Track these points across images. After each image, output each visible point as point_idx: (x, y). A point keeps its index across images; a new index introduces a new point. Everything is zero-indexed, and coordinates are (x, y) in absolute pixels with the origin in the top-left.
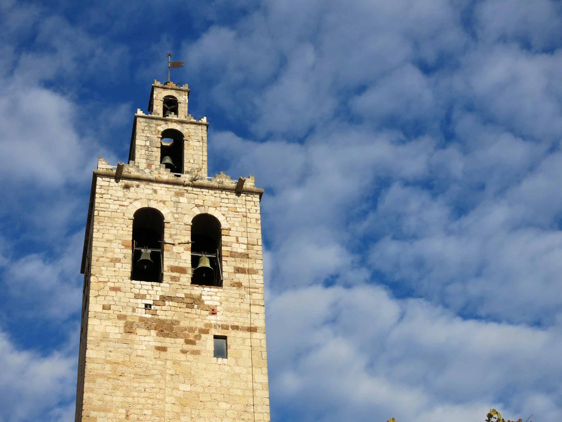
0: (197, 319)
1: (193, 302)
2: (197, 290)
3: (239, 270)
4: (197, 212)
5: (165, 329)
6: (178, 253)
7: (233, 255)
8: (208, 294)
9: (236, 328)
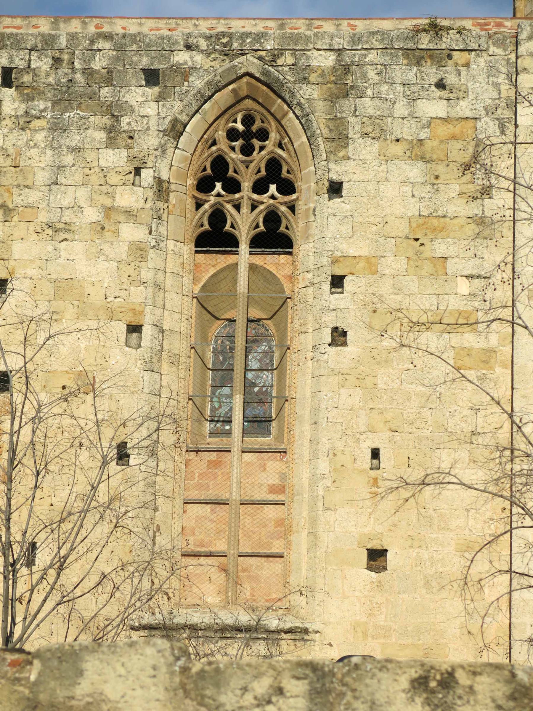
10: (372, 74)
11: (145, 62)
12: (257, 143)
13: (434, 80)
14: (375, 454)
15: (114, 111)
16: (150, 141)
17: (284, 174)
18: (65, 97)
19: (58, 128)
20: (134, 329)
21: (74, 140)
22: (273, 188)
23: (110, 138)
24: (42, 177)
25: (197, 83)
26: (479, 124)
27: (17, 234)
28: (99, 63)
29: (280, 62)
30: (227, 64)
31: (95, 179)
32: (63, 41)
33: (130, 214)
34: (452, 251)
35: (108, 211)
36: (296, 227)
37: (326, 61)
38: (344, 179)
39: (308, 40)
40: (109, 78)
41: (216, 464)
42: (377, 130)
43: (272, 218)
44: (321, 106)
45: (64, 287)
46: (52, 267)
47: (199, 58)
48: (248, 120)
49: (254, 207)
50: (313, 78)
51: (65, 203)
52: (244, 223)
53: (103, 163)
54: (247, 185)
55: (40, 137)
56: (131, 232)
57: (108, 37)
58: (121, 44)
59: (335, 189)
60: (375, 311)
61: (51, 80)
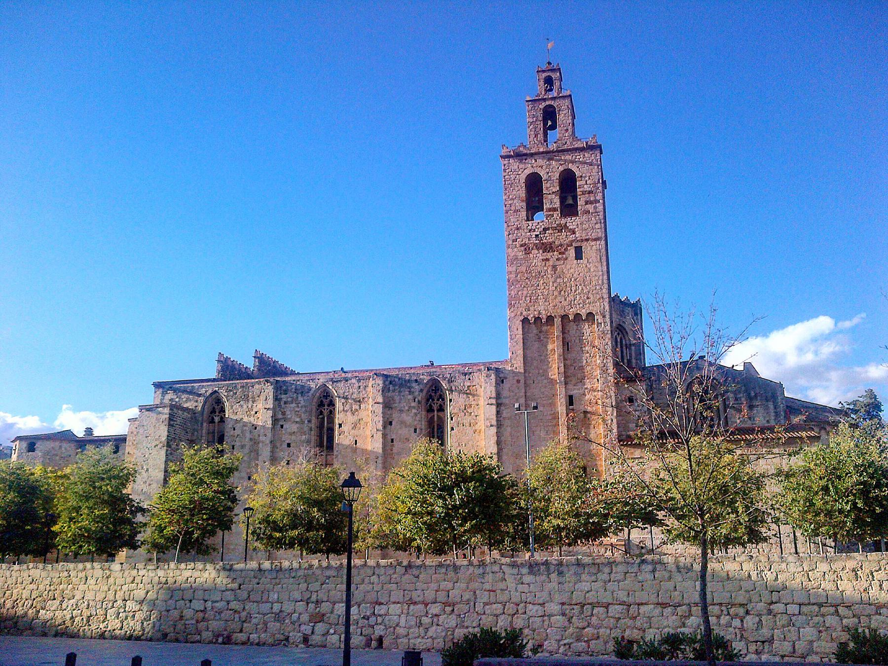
0: (564, 238)
1: (561, 228)
2: (563, 221)
3: (587, 203)
4: (561, 168)
5: (547, 248)
6: (552, 199)
7: (584, 193)
8: (572, 222)
9: (587, 240)
18: (401, 386)
20: (415, 430)
33: (414, 407)
35: (410, 407)
45: (403, 423)
52: (435, 407)
56: (414, 411)
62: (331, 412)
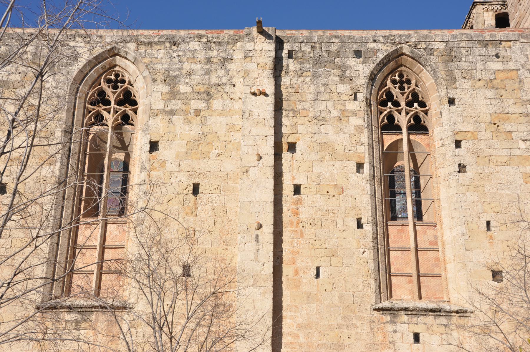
10: (464, 52)
11: (355, 47)
12: (406, 86)
13: (494, 54)
14: (488, 223)
15: (342, 68)
16: (362, 81)
17: (420, 99)
19: (315, 75)
21: (325, 80)
22: (416, 105)
23: (341, 80)
24: (310, 97)
25: (381, 56)
26: (519, 72)
27: (300, 122)
28: (334, 48)
29: (419, 47)
30: (394, 48)
31: (335, 98)
32: (316, 39)
33: (355, 113)
34: (514, 128)
35: (343, 111)
36: (431, 121)
37: (442, 46)
38: (455, 97)
39: (431, 38)
40: (338, 54)
41: (402, 231)
42: (468, 75)
43: (416, 117)
44: (441, 66)
46: (317, 137)
47: (380, 46)
48: (401, 76)
49: (407, 114)
50: (435, 53)
51: (322, 108)
53: (338, 91)
54: (403, 104)
55: (308, 80)
57: (336, 37)
58: (343, 41)
59: (451, 102)
60: (478, 157)
61: (311, 55)
62: (126, 119)
